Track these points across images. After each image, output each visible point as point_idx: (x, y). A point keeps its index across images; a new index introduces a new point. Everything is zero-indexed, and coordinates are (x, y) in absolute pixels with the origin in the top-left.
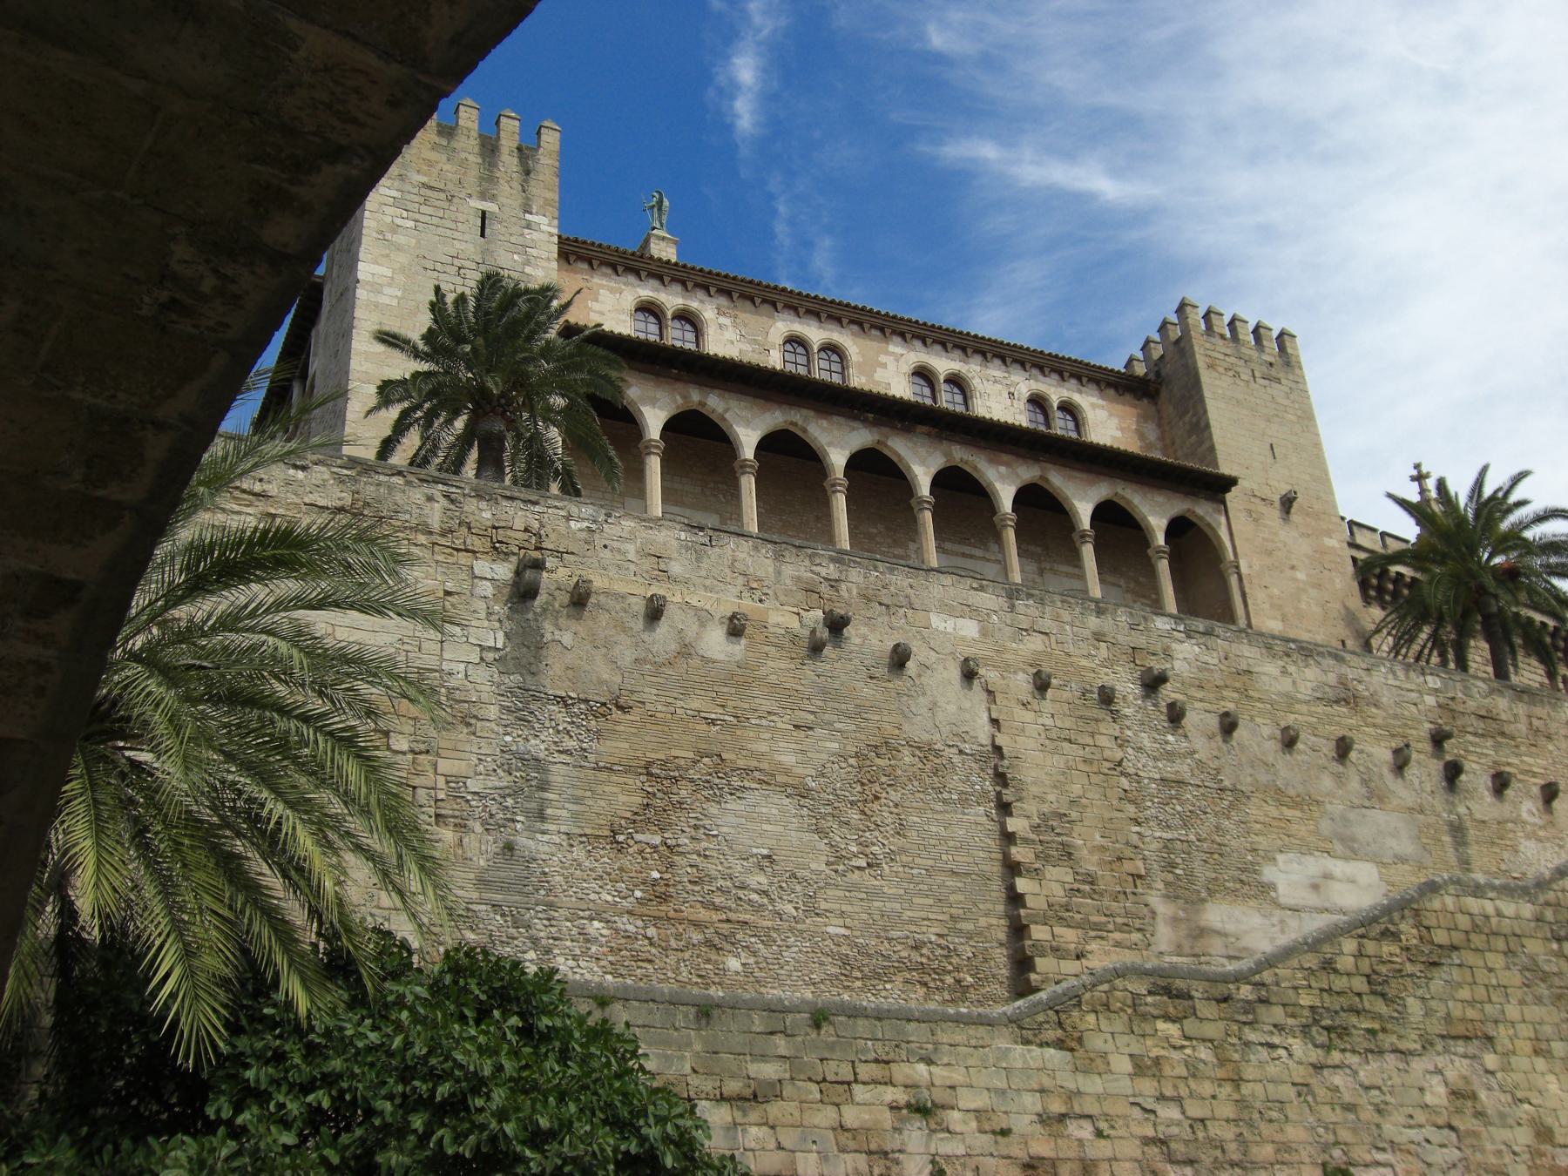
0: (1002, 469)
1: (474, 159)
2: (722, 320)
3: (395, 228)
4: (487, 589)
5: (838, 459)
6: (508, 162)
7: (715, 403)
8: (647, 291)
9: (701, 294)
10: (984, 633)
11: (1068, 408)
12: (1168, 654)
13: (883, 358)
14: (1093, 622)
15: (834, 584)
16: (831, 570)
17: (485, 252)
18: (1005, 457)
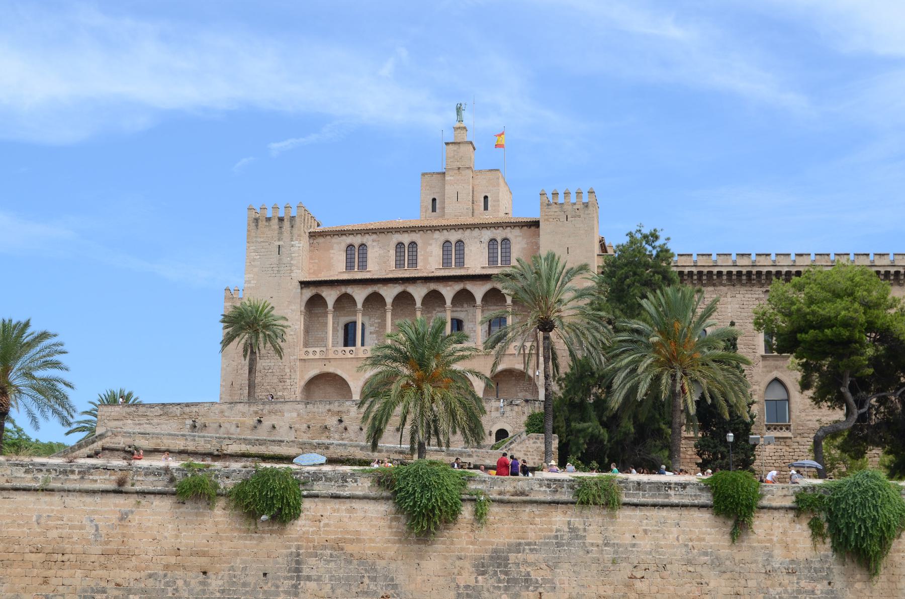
0: (448, 288)
1: (276, 227)
2: (375, 244)
3: (254, 260)
4: (188, 426)
5: (389, 300)
6: (287, 224)
7: (349, 290)
8: (349, 240)
9: (367, 236)
10: (298, 415)
11: (505, 240)
12: (348, 411)
13: (431, 242)
14: (328, 407)
15: (262, 410)
16: (261, 407)
17: (280, 259)
18: (450, 283)
